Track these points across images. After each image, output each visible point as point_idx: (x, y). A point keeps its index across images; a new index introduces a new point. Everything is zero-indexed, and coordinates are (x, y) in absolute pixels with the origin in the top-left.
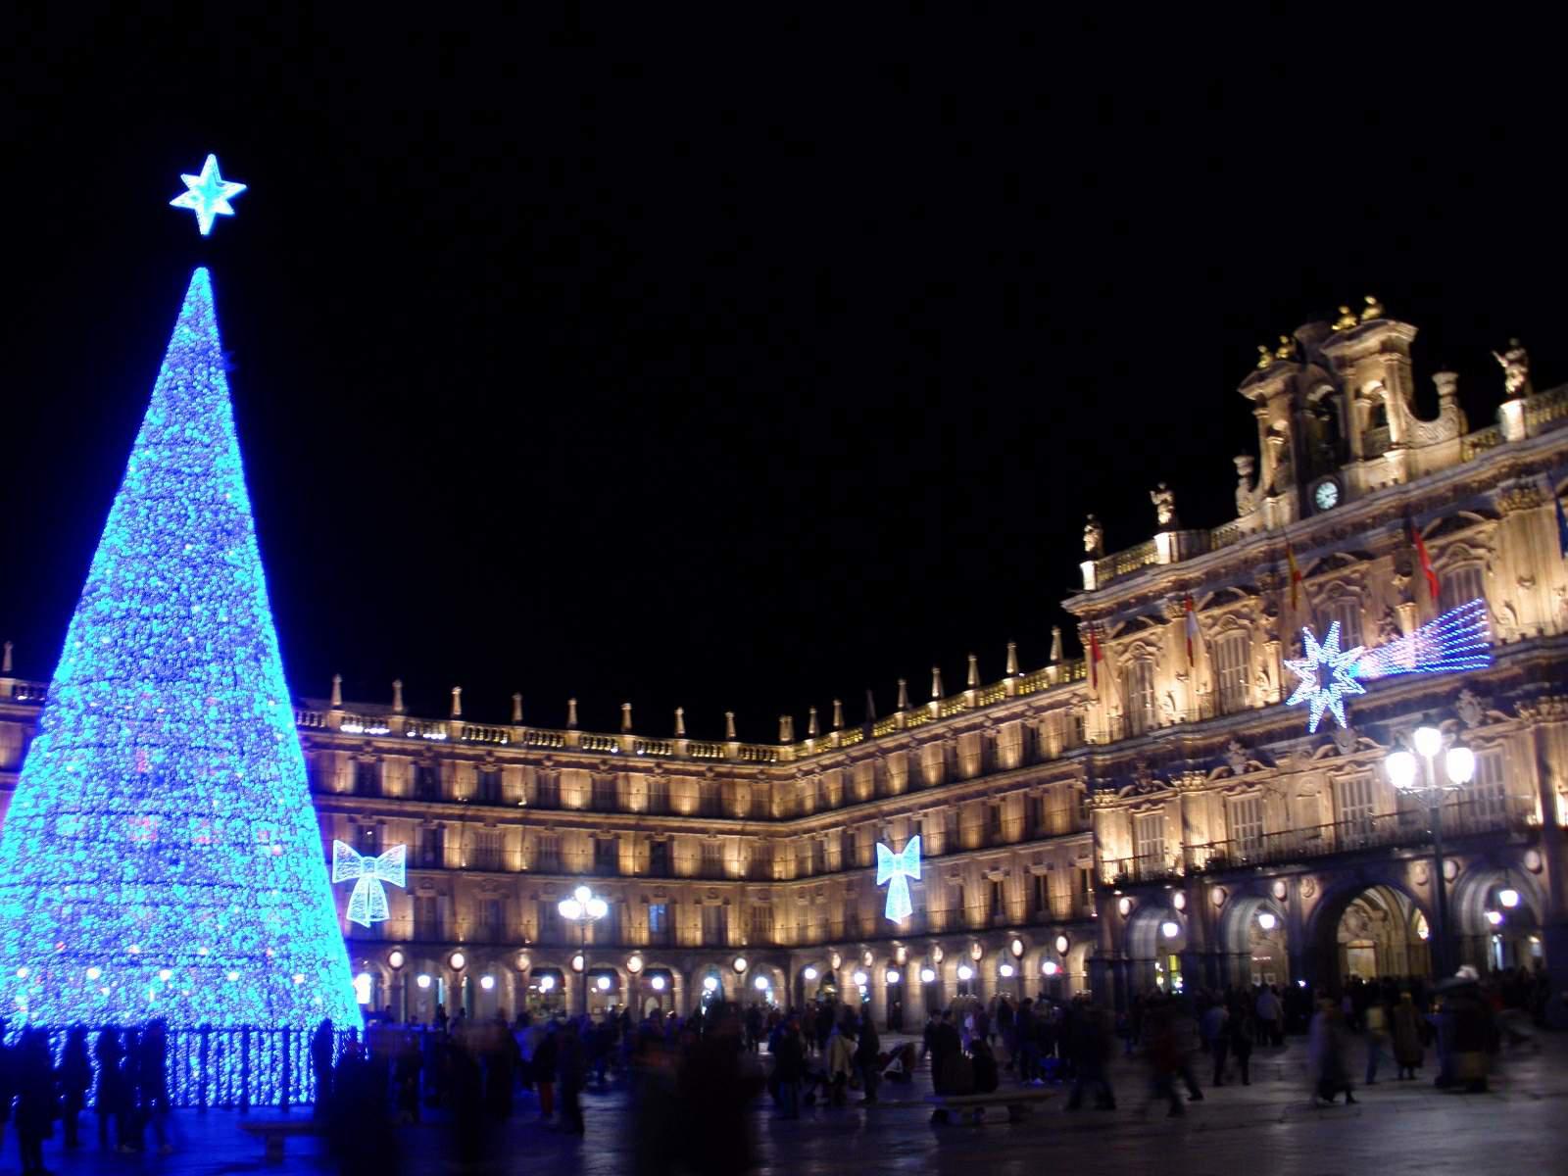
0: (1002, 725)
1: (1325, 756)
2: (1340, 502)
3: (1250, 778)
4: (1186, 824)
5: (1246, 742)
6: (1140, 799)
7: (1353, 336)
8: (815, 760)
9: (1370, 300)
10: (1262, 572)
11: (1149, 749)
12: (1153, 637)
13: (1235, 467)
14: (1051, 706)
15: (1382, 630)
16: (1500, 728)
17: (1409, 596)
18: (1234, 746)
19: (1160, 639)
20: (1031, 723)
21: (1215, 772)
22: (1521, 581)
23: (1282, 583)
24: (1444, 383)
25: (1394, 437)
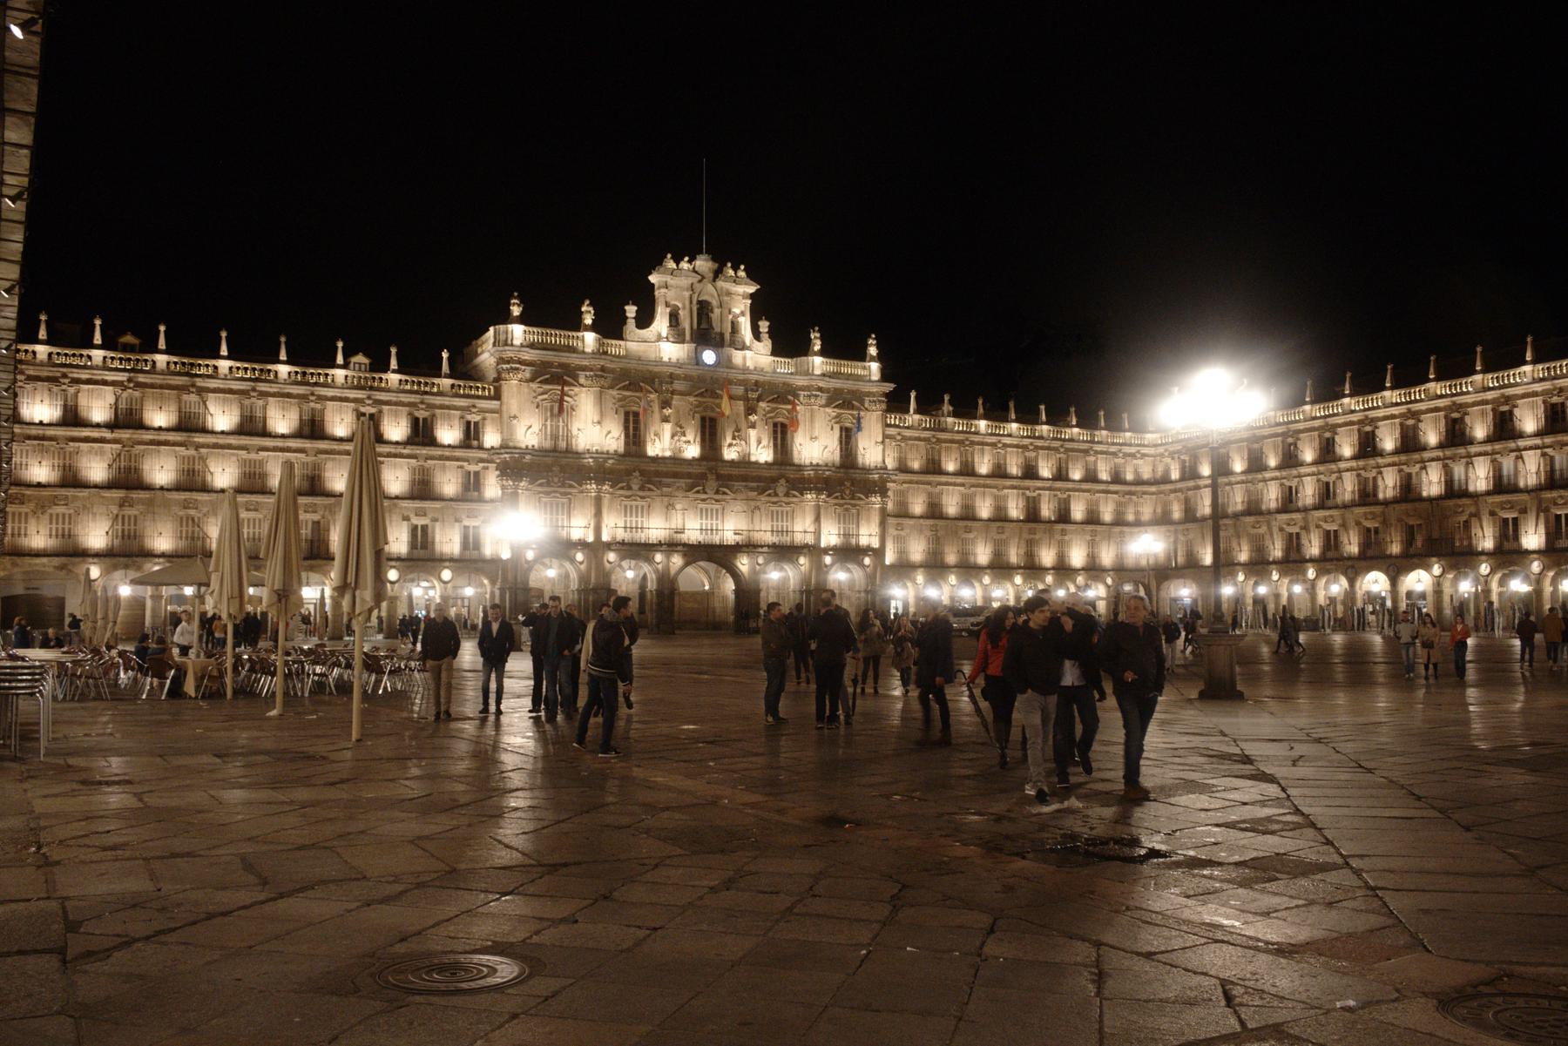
0: (385, 408)
1: (698, 492)
2: (718, 363)
3: (641, 493)
4: (598, 514)
5: (642, 473)
6: (552, 489)
7: (736, 281)
8: (64, 370)
9: (742, 267)
10: (667, 383)
11: (564, 461)
12: (570, 393)
13: (625, 311)
14: (442, 407)
15: (734, 438)
16: (794, 499)
17: (753, 426)
18: (637, 474)
19: (576, 395)
20: (421, 414)
21: (620, 485)
22: (816, 438)
23: (673, 393)
24: (764, 326)
25: (748, 343)
